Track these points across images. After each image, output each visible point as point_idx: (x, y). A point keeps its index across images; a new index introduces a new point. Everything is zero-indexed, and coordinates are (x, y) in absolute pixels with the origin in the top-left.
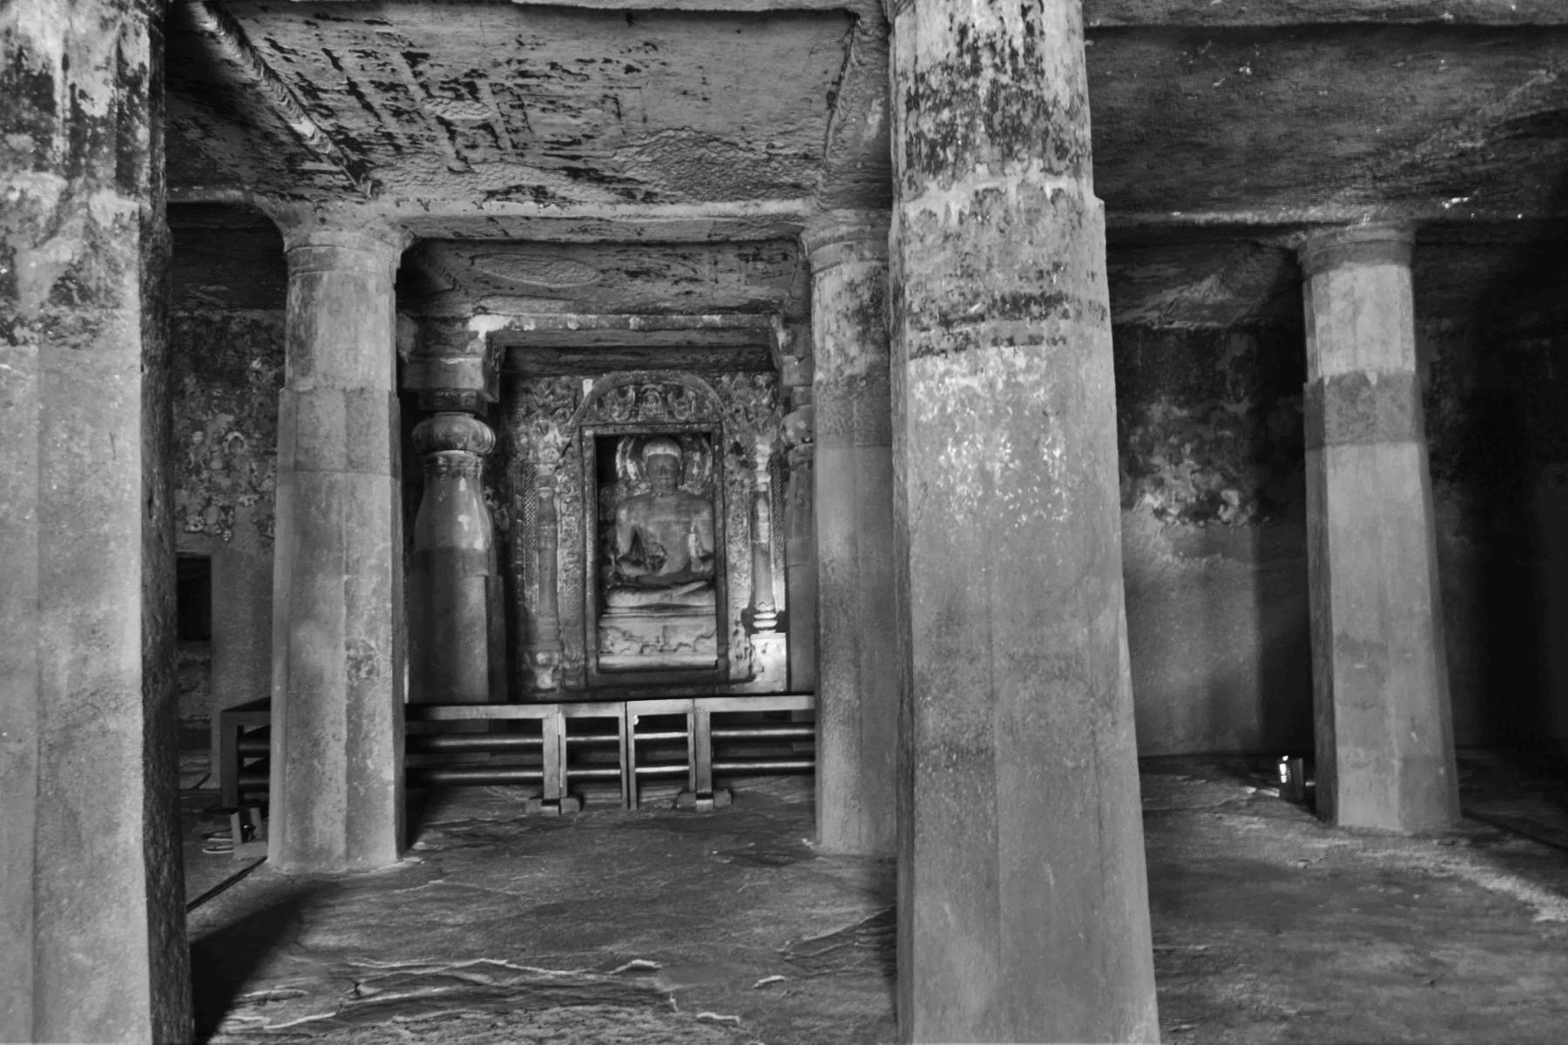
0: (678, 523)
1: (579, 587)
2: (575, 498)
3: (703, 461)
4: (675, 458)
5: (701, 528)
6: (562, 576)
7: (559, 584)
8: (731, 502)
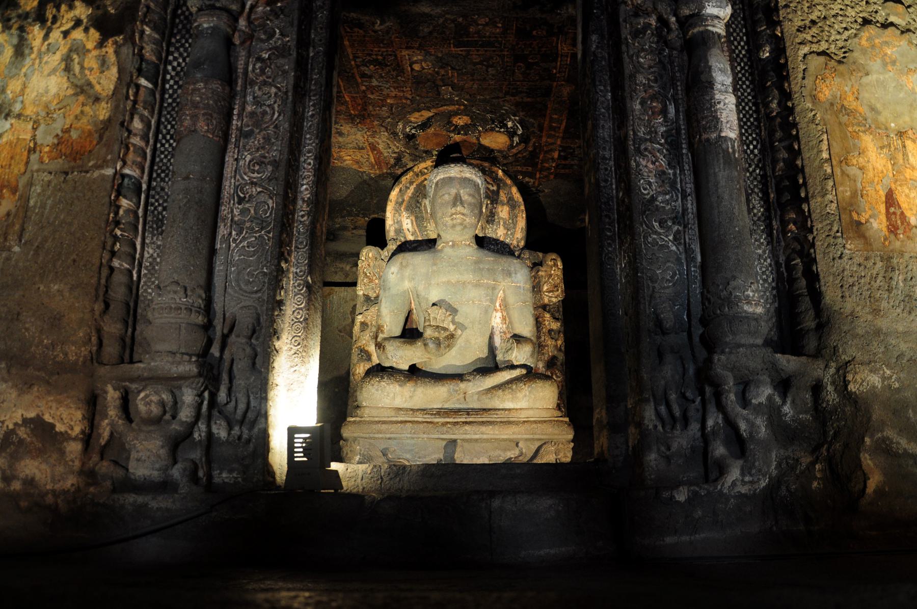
0: (477, 285)
1: (269, 236)
2: (281, 52)
3: (513, 217)
4: (476, 186)
5: (511, 300)
6: (230, 210)
7: (222, 231)
8: (638, 68)
